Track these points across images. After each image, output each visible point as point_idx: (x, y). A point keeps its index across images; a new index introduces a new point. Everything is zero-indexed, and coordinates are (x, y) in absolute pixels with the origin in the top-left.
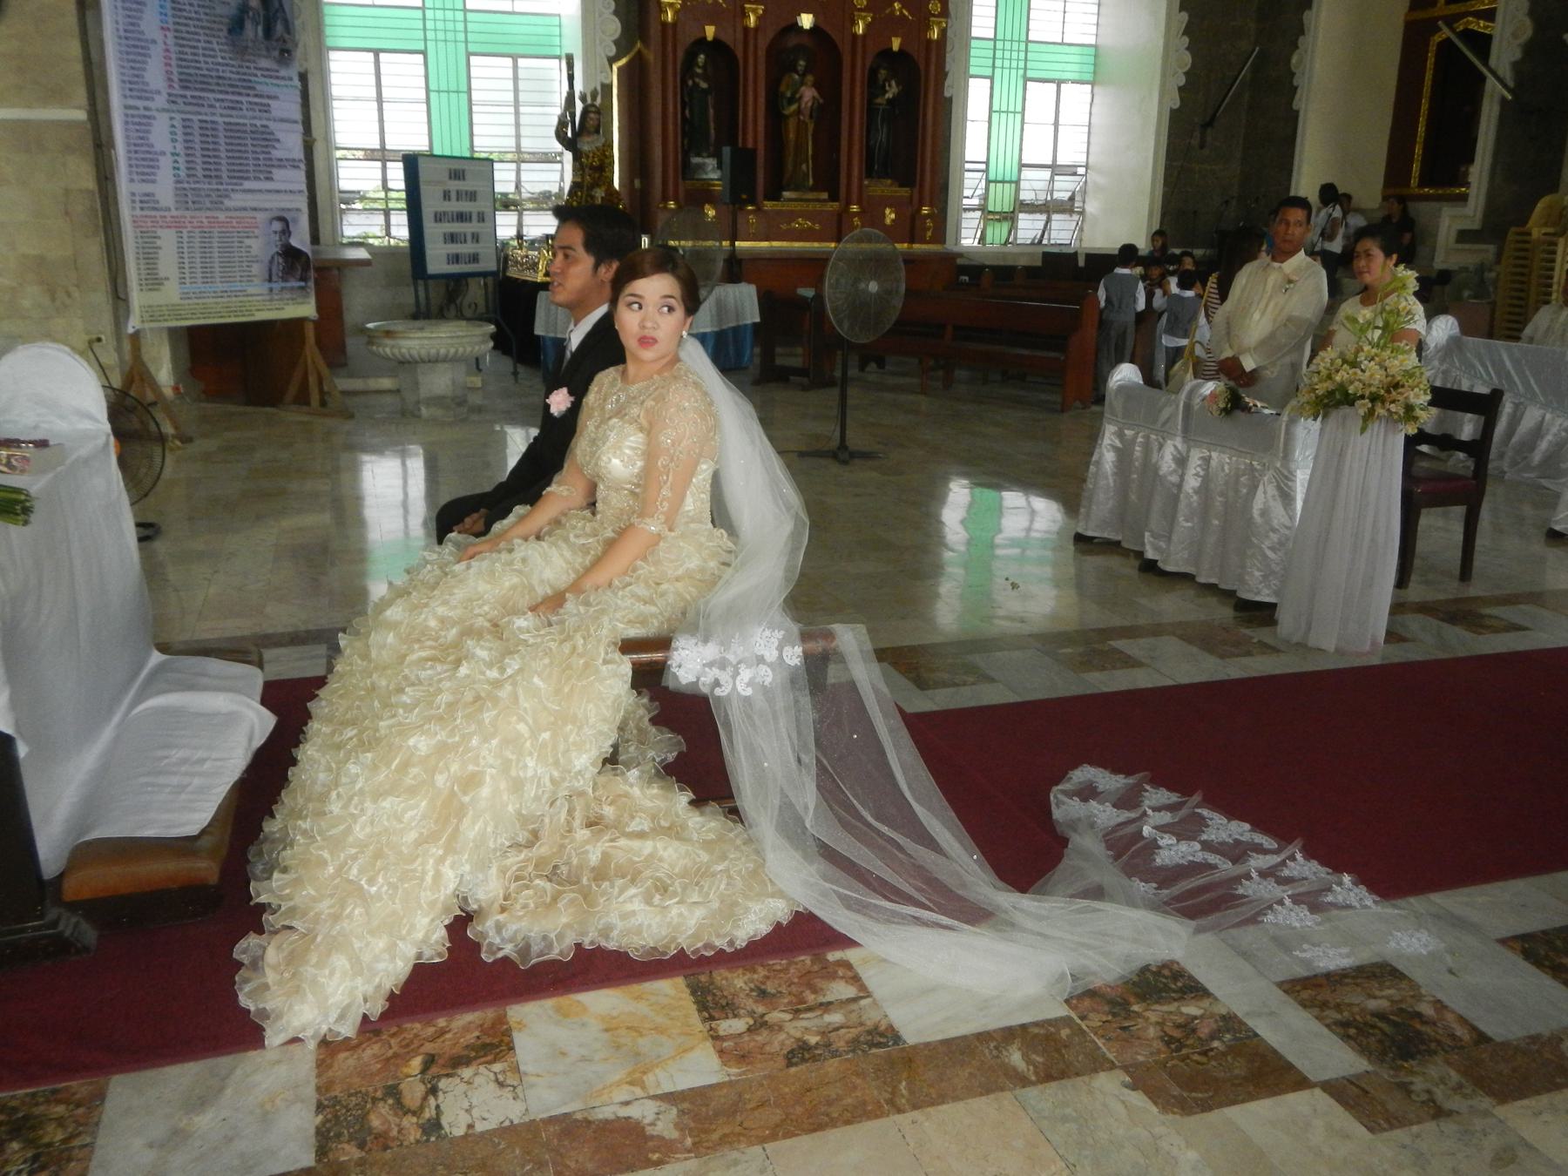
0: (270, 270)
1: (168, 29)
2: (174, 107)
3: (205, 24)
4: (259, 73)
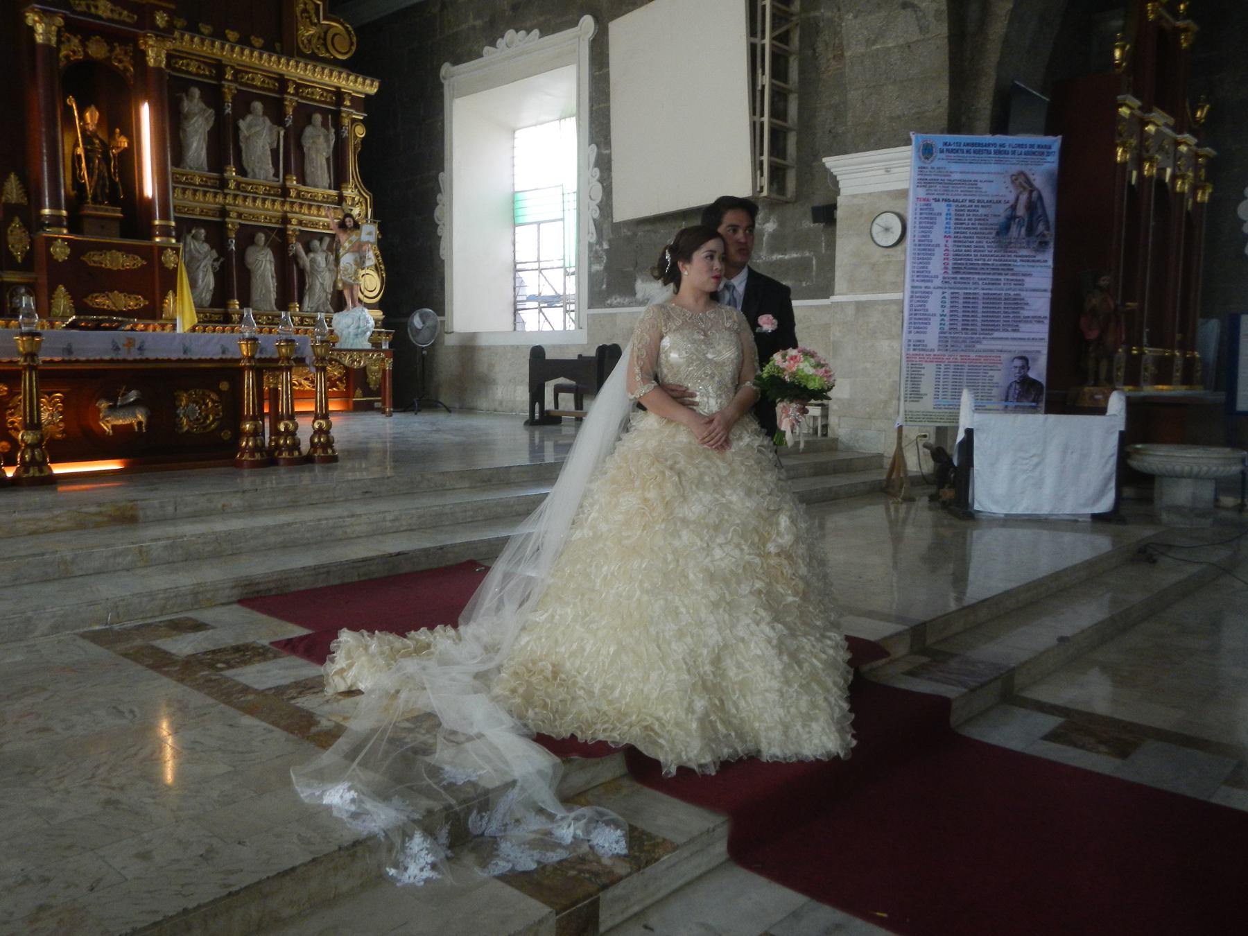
0: (1008, 393)
1: (950, 237)
2: (947, 285)
3: (979, 231)
4: (1018, 259)
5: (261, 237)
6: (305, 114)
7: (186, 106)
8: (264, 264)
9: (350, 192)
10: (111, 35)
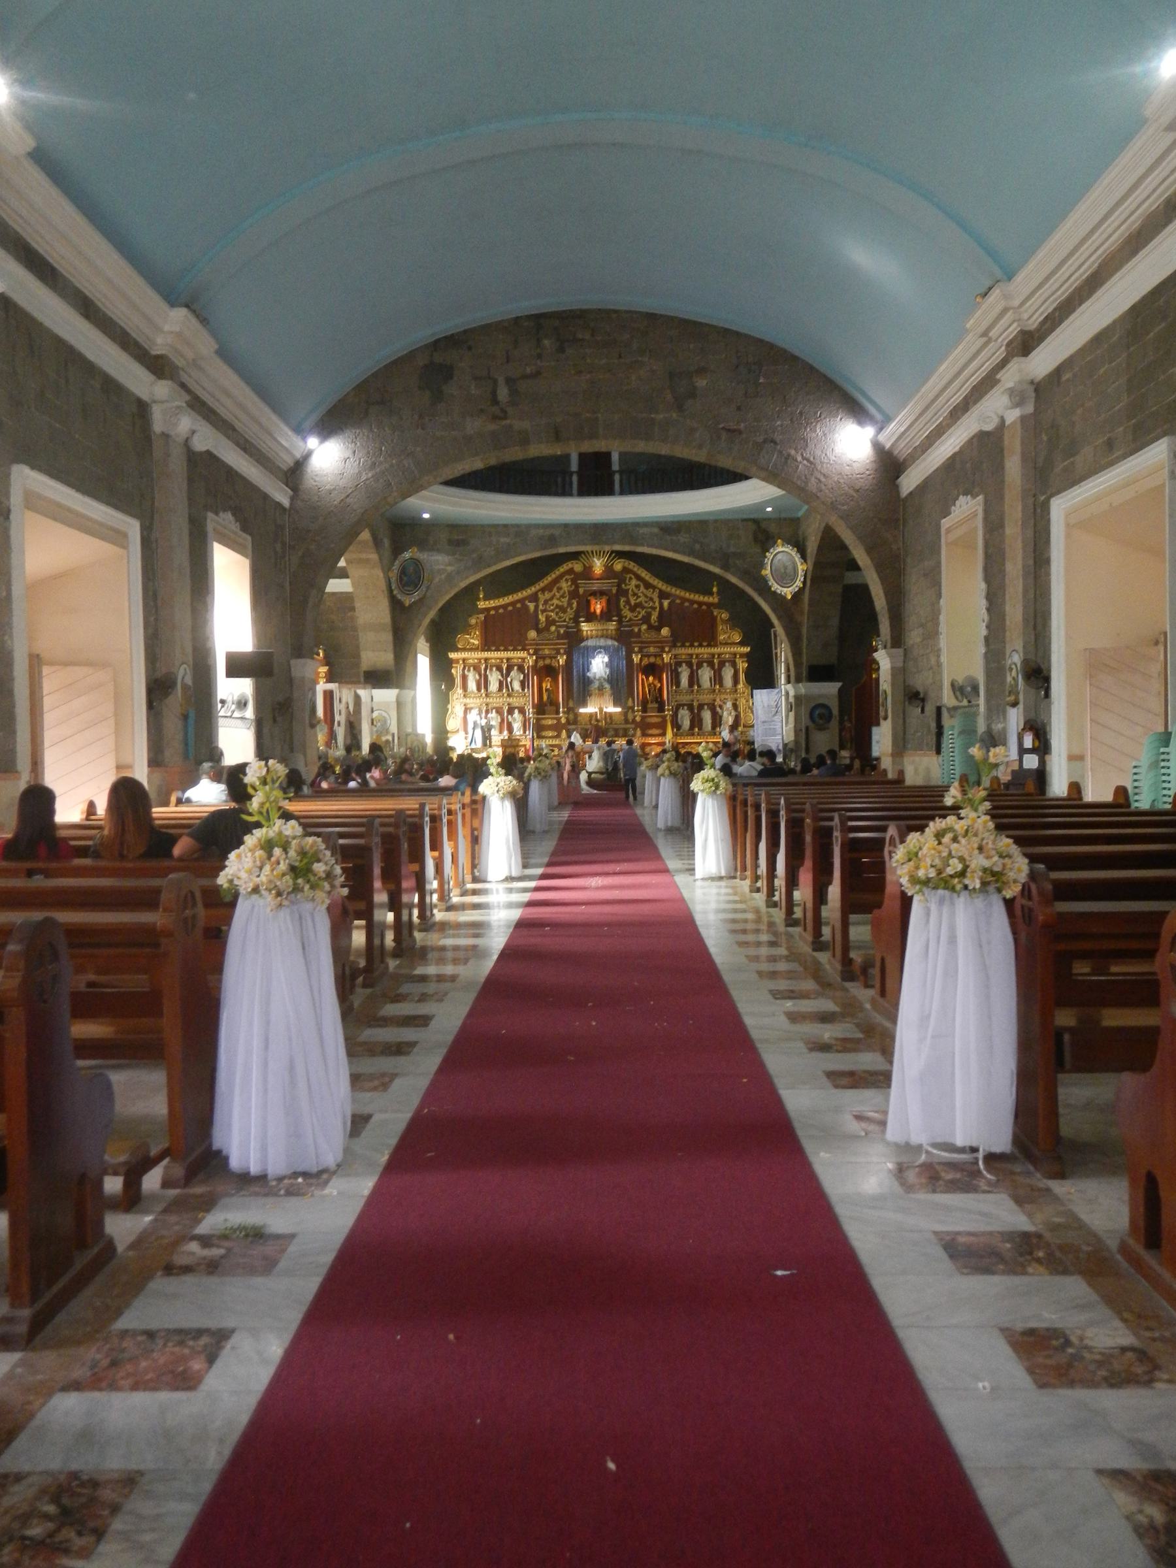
5: (706, 707)
6: (722, 664)
7: (680, 670)
8: (707, 716)
9: (740, 686)
10: (655, 656)
